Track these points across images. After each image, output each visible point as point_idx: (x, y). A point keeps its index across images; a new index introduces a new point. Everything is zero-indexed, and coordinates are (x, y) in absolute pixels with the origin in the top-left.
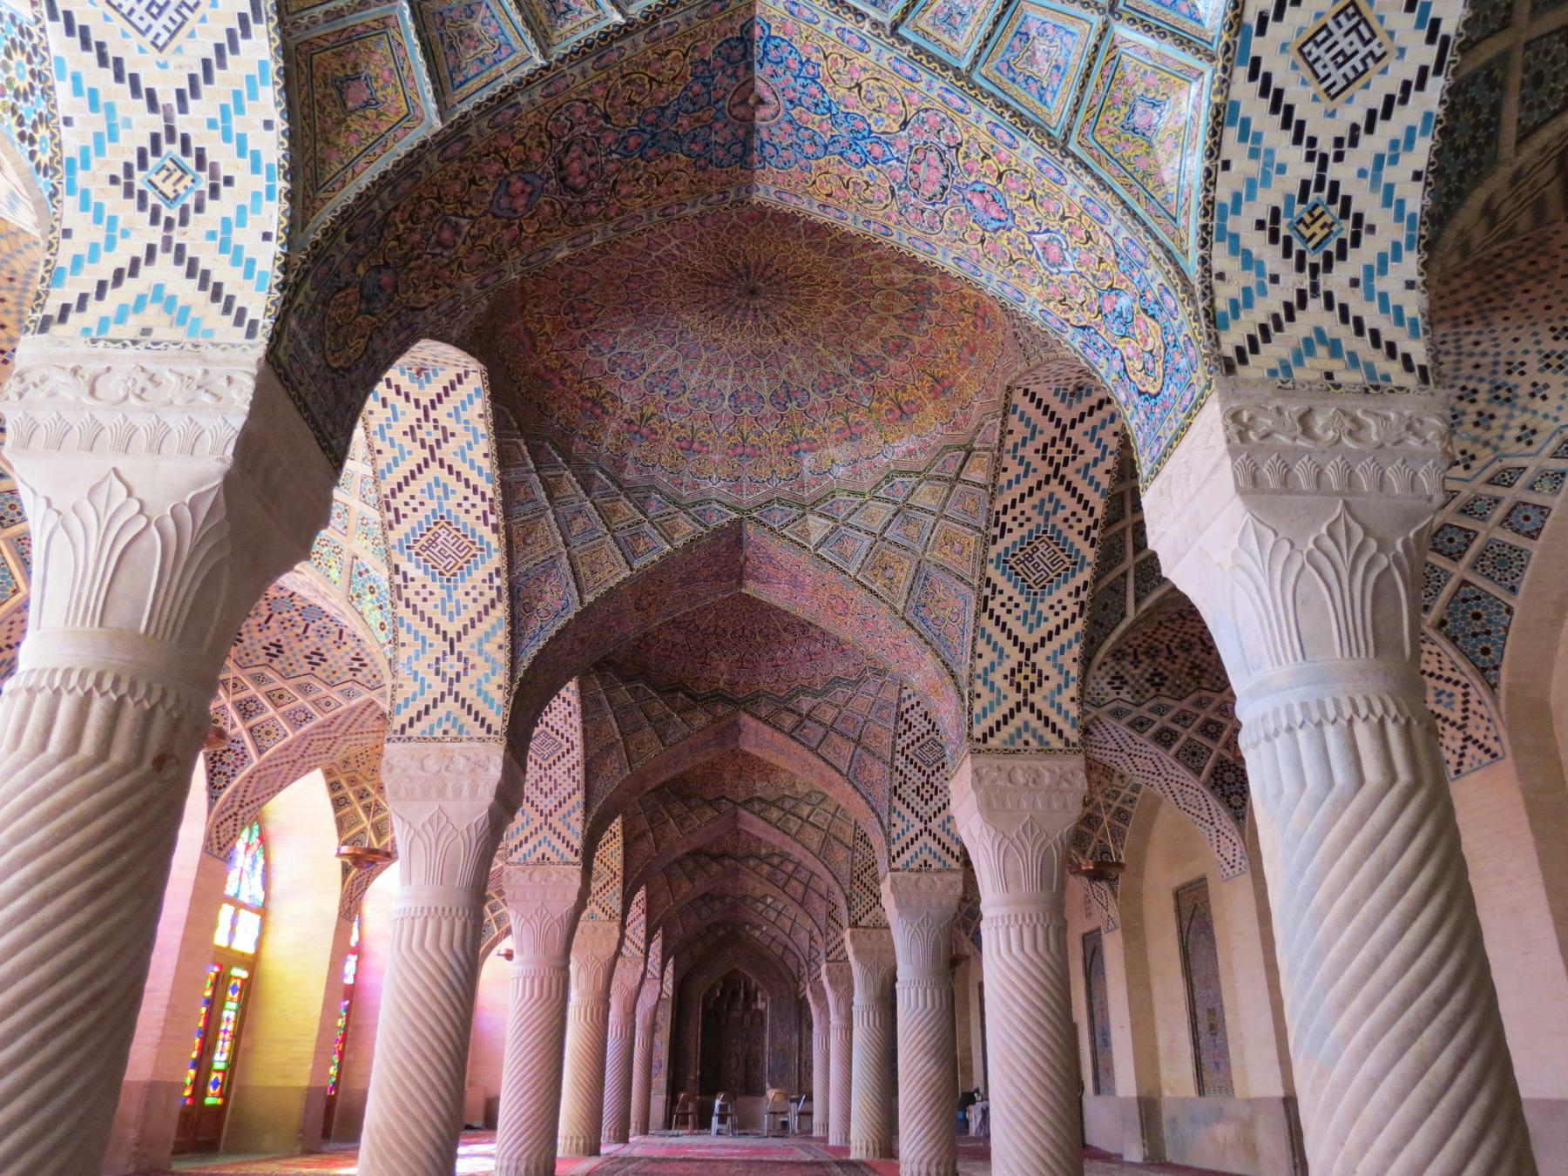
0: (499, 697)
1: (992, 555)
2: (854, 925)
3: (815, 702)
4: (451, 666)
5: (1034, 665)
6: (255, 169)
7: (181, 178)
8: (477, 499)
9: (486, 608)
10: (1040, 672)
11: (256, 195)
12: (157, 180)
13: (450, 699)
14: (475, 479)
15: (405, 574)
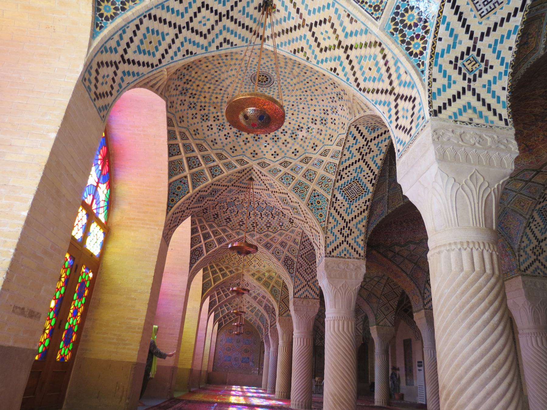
0: (362, 243)
1: (537, 208)
2: (377, 324)
3: (401, 249)
4: (346, 232)
5: (541, 246)
6: (502, 64)
7: (474, 64)
8: (371, 174)
9: (361, 212)
10: (543, 249)
11: (500, 73)
12: (466, 64)
13: (345, 243)
14: (373, 167)
15: (337, 198)
